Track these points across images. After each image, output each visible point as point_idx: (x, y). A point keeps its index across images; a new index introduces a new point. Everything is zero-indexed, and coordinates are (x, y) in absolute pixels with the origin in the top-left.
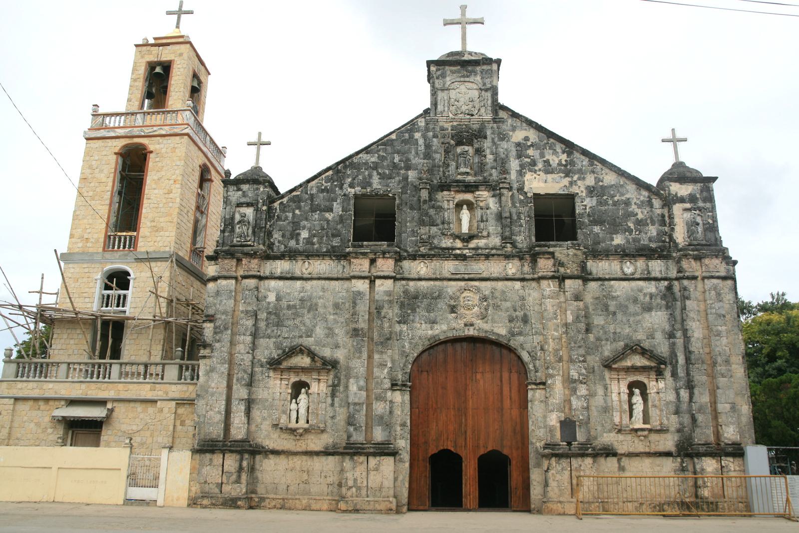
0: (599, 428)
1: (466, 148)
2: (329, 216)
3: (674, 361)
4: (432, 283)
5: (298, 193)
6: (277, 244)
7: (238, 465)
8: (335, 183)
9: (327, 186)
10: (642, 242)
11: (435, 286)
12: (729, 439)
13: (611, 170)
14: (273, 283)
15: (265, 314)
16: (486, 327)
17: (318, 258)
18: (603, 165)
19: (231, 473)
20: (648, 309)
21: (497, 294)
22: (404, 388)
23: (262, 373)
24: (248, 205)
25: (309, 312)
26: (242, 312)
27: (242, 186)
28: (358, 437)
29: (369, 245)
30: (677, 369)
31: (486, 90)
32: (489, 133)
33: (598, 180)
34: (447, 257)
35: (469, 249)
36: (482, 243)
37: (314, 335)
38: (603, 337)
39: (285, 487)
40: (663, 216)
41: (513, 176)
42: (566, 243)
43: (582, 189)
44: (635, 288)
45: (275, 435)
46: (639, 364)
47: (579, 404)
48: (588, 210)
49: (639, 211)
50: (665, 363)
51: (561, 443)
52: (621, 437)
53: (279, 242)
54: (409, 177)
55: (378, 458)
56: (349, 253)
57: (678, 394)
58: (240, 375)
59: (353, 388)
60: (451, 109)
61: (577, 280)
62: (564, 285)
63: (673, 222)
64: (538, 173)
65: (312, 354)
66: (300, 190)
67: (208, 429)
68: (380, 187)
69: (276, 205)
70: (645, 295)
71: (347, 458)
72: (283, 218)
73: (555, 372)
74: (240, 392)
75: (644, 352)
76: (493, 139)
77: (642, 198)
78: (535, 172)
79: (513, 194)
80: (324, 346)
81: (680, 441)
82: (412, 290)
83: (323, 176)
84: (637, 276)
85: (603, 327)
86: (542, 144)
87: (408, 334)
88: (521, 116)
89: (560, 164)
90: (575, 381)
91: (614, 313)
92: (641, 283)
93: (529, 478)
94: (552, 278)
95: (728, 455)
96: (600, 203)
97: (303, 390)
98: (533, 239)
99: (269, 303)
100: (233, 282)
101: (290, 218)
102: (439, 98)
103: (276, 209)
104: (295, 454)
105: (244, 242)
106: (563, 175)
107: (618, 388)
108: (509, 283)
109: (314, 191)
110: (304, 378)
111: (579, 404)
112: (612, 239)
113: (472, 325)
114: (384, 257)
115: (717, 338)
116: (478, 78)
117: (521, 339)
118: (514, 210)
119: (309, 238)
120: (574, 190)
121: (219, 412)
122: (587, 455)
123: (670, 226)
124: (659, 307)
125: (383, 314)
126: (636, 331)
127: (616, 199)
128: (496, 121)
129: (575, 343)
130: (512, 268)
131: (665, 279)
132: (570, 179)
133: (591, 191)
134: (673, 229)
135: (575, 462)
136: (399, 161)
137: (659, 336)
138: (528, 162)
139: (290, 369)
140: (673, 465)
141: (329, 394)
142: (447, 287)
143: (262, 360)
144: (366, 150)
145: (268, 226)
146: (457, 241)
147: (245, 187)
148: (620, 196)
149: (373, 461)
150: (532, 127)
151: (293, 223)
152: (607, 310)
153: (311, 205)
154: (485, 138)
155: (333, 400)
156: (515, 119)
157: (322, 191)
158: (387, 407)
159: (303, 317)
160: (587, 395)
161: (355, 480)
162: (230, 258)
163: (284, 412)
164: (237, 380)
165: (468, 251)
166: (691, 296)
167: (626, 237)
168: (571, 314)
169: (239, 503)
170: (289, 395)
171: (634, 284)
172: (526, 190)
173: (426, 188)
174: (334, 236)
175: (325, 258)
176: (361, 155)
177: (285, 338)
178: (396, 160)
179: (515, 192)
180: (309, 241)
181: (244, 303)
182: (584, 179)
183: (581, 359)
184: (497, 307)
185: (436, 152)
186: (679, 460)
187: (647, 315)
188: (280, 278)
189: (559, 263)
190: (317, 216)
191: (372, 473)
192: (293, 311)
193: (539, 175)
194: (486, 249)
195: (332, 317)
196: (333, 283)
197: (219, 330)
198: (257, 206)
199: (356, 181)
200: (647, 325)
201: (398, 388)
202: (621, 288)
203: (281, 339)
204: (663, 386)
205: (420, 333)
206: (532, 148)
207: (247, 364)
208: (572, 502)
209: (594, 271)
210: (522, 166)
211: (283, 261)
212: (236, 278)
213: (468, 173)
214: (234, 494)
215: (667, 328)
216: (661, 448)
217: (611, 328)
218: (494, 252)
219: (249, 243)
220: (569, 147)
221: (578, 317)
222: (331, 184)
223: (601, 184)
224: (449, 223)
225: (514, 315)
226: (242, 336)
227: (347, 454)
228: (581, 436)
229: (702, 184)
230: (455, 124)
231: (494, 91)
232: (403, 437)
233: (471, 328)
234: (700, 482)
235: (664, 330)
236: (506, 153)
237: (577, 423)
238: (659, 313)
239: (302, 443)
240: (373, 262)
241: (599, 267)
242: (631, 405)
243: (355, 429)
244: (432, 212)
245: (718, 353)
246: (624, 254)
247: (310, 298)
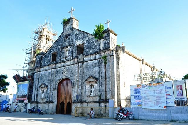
0: (84, 96)
2: (49, 58)
16: (67, 76)
20: (95, 67)
33: (88, 38)
52: (88, 98)
92: (94, 61)
94: (77, 63)
96: (88, 44)
107: (88, 87)
108: (71, 66)
112: (90, 52)
113: (65, 76)
120: (84, 42)
122: (79, 103)
124: (97, 66)
126: (92, 73)
131: (99, 59)
137: (97, 73)
149: (49, 104)
171: (92, 61)
184: (69, 71)
186: (99, 103)
188: (42, 71)
210: (76, 40)
215: (99, 71)
216: (95, 101)
228: (79, 99)
241: (86, 59)
246: (91, 54)
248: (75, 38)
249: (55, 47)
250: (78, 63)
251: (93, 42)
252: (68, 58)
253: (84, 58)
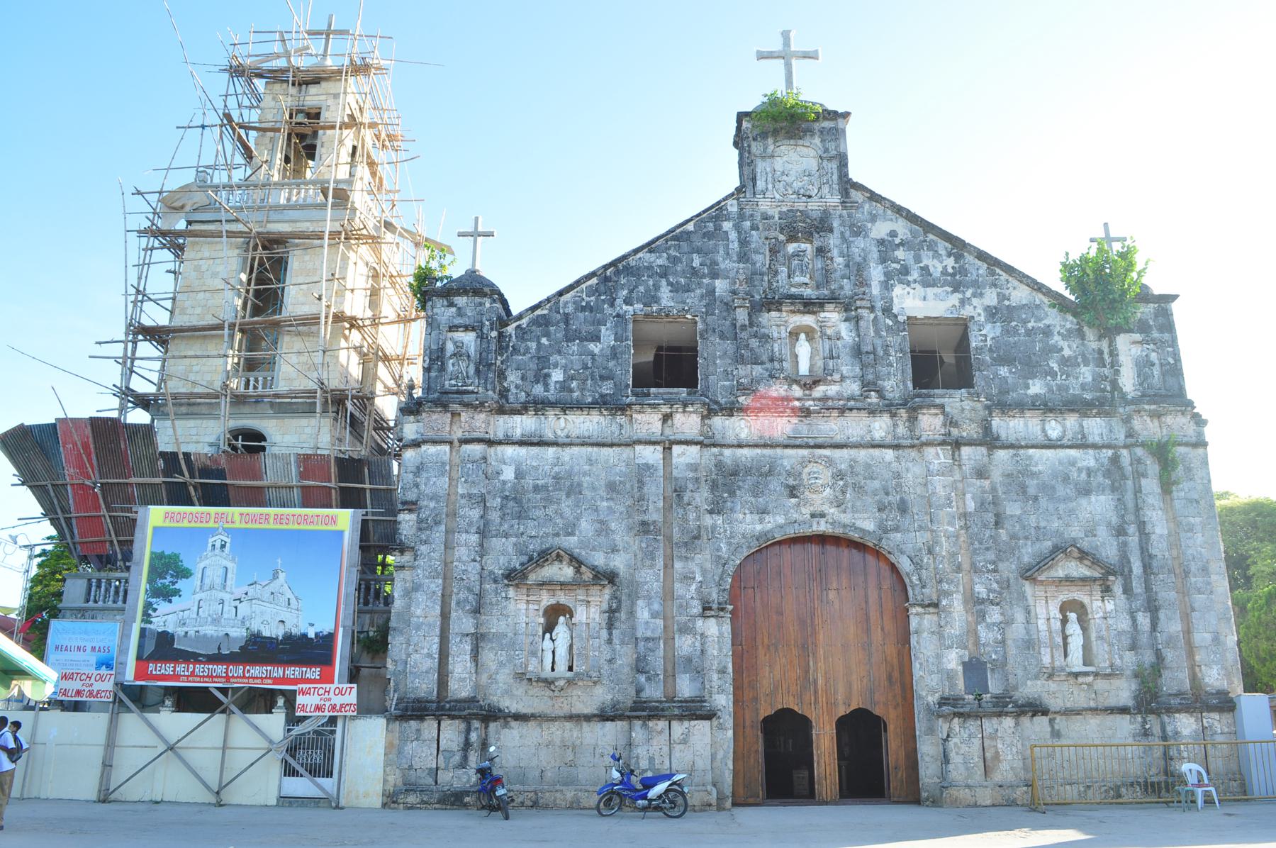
0: (1020, 673)
1: (803, 246)
2: (595, 348)
3: (1126, 570)
4: (758, 451)
5: (545, 312)
6: (514, 390)
7: (463, 739)
8: (603, 298)
9: (590, 301)
10: (1071, 391)
11: (764, 456)
12: (1212, 686)
13: (1021, 282)
14: (509, 451)
15: (499, 500)
16: (846, 518)
17: (580, 412)
18: (1010, 275)
19: (452, 753)
20: (1085, 491)
21: (859, 469)
22: (722, 614)
23: (497, 593)
24: (467, 328)
25: (568, 496)
26: (463, 496)
27: (456, 298)
28: (654, 692)
29: (659, 394)
30: (1131, 582)
31: (830, 159)
32: (836, 224)
33: (1003, 298)
34: (781, 412)
35: (814, 400)
36: (832, 390)
37: (577, 533)
38: (1021, 534)
39: (537, 773)
40: (1101, 352)
41: (875, 290)
42: (960, 391)
43: (979, 310)
44: (1065, 461)
45: (520, 690)
46: (1075, 574)
48: (989, 343)
49: (1064, 344)
50: (1114, 573)
51: (966, 697)
52: (1053, 686)
53: (517, 387)
54: (717, 290)
55: (686, 724)
56: (630, 405)
57: (1134, 620)
58: (462, 596)
59: (643, 614)
60: (777, 187)
61: (978, 448)
62: (959, 455)
63: (1117, 362)
64: (912, 285)
65: (577, 562)
66: (547, 307)
67: (412, 682)
68: (673, 304)
69: (511, 329)
70: (1080, 470)
71: (638, 723)
72: (522, 351)
73: (952, 588)
74: (463, 623)
75: (1083, 555)
76: (842, 233)
77: (1068, 326)
78: (908, 284)
79: (875, 317)
80: (594, 549)
81: (1140, 690)
82: (729, 462)
83: (584, 286)
84: (1065, 441)
85: (1020, 519)
86: (917, 241)
87: (726, 531)
88: (885, 199)
89: (944, 272)
90: (982, 601)
91: (1036, 498)
92: (1073, 452)
93: (915, 750)
95: (1211, 709)
96: (1006, 332)
97: (562, 619)
98: (910, 385)
99: (504, 483)
100: (447, 448)
101: (533, 351)
102: (759, 170)
103: (510, 335)
104: (554, 719)
105: (462, 386)
106: (950, 289)
107: (1046, 610)
108: (876, 452)
109: (570, 309)
110: (563, 598)
111: (990, 635)
112: (1027, 387)
113: (823, 515)
114: (684, 412)
115: (1189, 534)
116: (817, 140)
117: (898, 536)
118: (878, 342)
119: (564, 381)
120: (967, 311)
121: (430, 656)
122: (1007, 714)
123: (1112, 367)
124: (1101, 489)
125: (686, 499)
126: (1068, 525)
127: (1030, 325)
128: (846, 207)
129: (981, 543)
130: (880, 427)
131: (1108, 447)
132: (961, 296)
133: (992, 313)
134: (1117, 372)
135: (989, 725)
136: (701, 265)
137: (1103, 534)
138: (896, 269)
139: (542, 584)
140: (1132, 727)
141: (604, 625)
142: (782, 458)
143: (496, 571)
144: (650, 246)
145: (498, 363)
146: (795, 387)
147: (461, 301)
148: (1035, 322)
149: (678, 728)
150: (901, 215)
151: (539, 358)
152: (1024, 493)
153: (566, 330)
154: (831, 231)
155: (610, 634)
156: (874, 203)
157: (583, 309)
158: (698, 644)
159: (559, 504)
160: (1001, 623)
161: (651, 759)
162: (441, 412)
163: (534, 654)
164: (458, 603)
165: (811, 403)
166: (1149, 472)
167: (1048, 384)
168: (973, 499)
169: (467, 799)
170: (541, 626)
172: (895, 311)
173: (745, 307)
174: (602, 378)
175: (591, 413)
176: (640, 255)
177: (531, 537)
178: (696, 263)
179: (880, 314)
180: (564, 386)
181: (466, 481)
182: (981, 295)
183: (991, 567)
184: (859, 489)
185: (757, 252)
186: (1139, 719)
187: (1083, 502)
188: (522, 443)
189: (951, 422)
190: (575, 348)
191: (677, 748)
192: (543, 495)
193: (914, 289)
194: (839, 400)
195: (605, 504)
196: (606, 451)
197: (426, 525)
198: (481, 330)
199: (634, 295)
200: (1083, 515)
201: (713, 613)
202: (1044, 460)
203: (525, 538)
204: (1113, 607)
205: (742, 528)
206: (901, 248)
207: (472, 579)
208: (987, 787)
209: (1003, 436)
210: (888, 275)
211: (524, 417)
212: (451, 443)
213: (806, 284)
214: (457, 785)
215: (1115, 520)
216: (1112, 702)
217: (1032, 520)
218: (852, 403)
219: (470, 388)
220: (958, 246)
221: (982, 504)
222: (597, 299)
223: (1007, 303)
224: (781, 361)
225: (886, 501)
226: (464, 535)
227: (638, 718)
228: (994, 686)
229: (1156, 305)
230: (785, 209)
231: (842, 161)
232: (723, 691)
233: (822, 521)
234: (1173, 752)
236: (862, 254)
237: (989, 666)
238: (1102, 498)
239: (562, 703)
240: (667, 418)
241: (1010, 426)
242: (1065, 638)
243: (649, 679)
244: (754, 343)
245: (1191, 558)
246: (1046, 407)
247: (570, 474)
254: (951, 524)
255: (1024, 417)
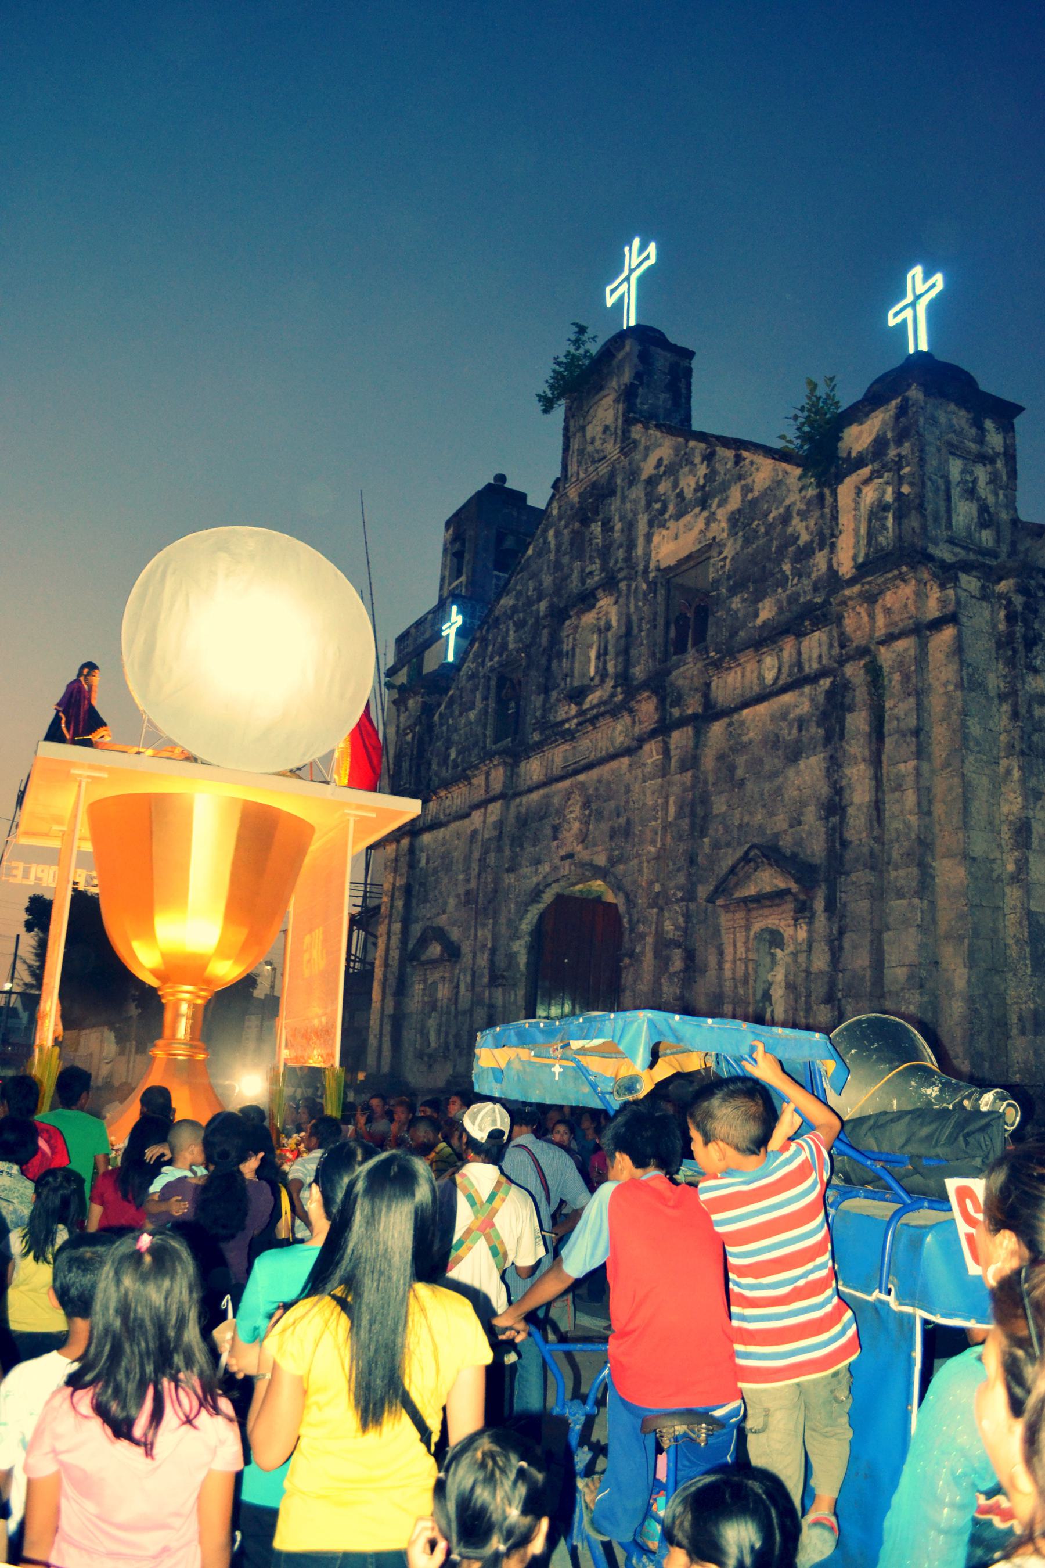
2: (472, 715)
20: (794, 754)
33: (747, 489)
47: (671, 990)
91: (742, 783)
92: (787, 698)
94: (653, 734)
96: (747, 541)
108: (614, 764)
112: (756, 615)
115: (897, 794)
126: (772, 814)
137: (811, 816)
184: (599, 814)
210: (651, 524)
235: (818, 799)
245: (894, 835)
248: (648, 505)
249: (511, 618)
250: (663, 728)
251: (785, 519)
252: (598, 693)
253: (708, 685)
254: (653, 842)
255: (740, 665)
